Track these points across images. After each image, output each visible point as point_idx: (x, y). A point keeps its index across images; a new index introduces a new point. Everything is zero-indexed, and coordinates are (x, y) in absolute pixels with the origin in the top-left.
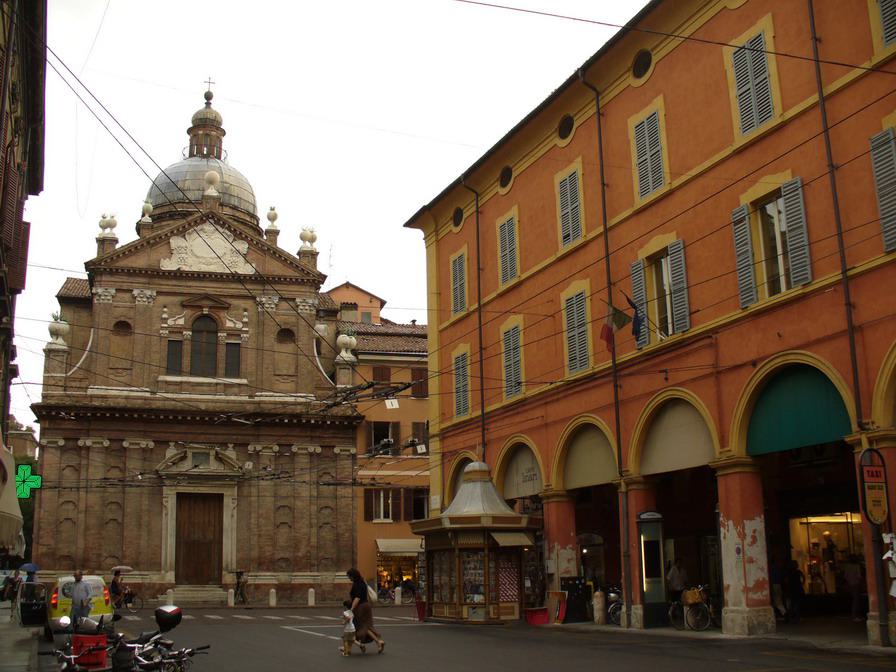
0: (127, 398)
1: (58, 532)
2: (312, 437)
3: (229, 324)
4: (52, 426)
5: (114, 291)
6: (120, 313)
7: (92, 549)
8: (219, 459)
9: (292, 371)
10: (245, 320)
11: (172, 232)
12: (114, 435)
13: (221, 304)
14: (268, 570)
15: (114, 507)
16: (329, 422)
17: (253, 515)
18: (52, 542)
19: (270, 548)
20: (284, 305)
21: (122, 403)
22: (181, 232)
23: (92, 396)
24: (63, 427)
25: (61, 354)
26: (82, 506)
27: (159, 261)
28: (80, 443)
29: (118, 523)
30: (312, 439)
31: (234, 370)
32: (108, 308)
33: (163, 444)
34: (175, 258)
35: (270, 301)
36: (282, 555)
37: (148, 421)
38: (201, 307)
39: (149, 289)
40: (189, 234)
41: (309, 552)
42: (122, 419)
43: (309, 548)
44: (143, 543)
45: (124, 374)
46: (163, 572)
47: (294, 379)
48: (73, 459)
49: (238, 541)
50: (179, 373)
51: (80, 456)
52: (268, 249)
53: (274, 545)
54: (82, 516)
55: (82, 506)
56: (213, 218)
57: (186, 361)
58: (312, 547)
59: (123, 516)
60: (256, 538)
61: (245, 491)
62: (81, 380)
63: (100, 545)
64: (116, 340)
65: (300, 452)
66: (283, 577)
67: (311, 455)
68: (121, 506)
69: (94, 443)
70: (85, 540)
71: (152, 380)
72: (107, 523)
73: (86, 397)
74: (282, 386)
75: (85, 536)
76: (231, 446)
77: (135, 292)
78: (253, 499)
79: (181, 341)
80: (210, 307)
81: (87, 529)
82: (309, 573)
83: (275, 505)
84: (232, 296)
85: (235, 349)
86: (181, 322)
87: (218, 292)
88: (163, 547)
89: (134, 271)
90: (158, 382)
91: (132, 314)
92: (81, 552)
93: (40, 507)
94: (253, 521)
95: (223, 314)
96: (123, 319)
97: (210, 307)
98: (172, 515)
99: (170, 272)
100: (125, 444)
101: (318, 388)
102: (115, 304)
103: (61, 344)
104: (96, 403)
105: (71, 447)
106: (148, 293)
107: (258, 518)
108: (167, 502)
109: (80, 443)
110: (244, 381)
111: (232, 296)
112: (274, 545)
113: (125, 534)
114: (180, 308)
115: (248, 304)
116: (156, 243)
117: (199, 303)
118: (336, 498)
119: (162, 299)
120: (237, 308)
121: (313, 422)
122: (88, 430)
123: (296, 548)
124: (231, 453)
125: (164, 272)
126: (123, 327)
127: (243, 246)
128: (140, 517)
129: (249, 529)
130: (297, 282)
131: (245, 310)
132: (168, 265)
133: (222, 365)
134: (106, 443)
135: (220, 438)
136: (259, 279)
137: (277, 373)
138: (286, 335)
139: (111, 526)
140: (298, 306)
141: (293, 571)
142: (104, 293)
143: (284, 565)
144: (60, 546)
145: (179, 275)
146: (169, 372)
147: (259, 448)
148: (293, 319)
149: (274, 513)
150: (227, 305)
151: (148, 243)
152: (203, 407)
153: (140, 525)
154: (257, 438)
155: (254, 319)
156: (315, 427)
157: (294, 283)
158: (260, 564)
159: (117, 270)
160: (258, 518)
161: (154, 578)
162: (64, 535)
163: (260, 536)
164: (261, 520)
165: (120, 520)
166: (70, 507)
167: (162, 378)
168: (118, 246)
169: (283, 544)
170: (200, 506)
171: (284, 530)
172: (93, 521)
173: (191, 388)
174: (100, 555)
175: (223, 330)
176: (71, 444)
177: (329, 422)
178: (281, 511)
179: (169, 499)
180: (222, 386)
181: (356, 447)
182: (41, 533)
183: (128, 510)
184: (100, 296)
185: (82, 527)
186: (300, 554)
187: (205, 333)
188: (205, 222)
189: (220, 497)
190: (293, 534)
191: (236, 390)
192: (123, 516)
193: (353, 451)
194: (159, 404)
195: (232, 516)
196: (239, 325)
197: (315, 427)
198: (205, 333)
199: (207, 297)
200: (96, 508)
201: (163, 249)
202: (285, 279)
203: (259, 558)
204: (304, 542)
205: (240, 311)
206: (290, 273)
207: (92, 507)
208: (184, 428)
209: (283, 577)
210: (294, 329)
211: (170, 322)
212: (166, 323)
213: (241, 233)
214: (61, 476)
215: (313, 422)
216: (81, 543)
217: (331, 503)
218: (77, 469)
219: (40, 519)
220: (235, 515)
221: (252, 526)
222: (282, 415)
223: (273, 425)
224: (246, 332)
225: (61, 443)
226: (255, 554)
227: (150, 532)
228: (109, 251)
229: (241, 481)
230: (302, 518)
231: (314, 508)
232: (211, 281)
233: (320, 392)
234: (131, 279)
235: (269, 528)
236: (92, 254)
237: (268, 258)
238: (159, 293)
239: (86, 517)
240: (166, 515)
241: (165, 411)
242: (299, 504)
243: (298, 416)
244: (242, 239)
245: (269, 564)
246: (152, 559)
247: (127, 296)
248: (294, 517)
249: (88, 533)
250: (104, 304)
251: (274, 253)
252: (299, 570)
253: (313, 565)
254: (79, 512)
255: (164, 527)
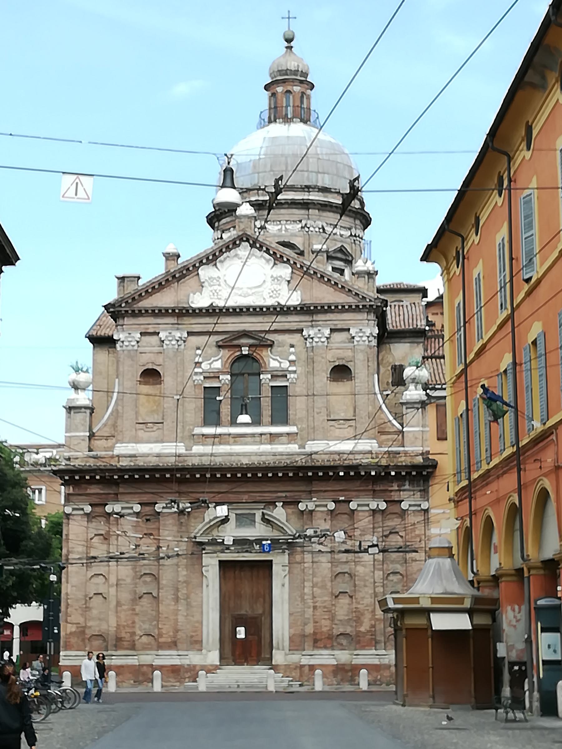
0: (158, 455)
1: (87, 608)
2: (374, 491)
3: (274, 364)
4: (77, 491)
5: (139, 335)
6: (147, 360)
7: (124, 626)
8: (266, 521)
9: (350, 416)
10: (292, 357)
11: (201, 261)
12: (145, 498)
13: (262, 342)
14: (325, 647)
15: (148, 579)
16: (393, 473)
17: (308, 584)
18: (81, 620)
19: (328, 623)
20: (338, 337)
21: (153, 462)
22: (212, 261)
23: (118, 456)
24: (89, 491)
25: (83, 410)
26: (113, 579)
27: (189, 296)
28: (108, 509)
29: (155, 597)
30: (375, 494)
31: (281, 416)
32: (133, 355)
33: (200, 505)
34: (206, 291)
35: (318, 332)
36: (341, 630)
37: (182, 481)
38: (240, 347)
39: (178, 329)
40: (221, 262)
41: (373, 626)
42: (153, 480)
43: (373, 622)
44: (181, 619)
45: (155, 428)
46: (204, 651)
47: (352, 423)
48: (100, 526)
49: (291, 614)
50: (218, 423)
51: (108, 521)
52: (315, 273)
53: (332, 618)
54: (113, 591)
55: (113, 579)
56: (248, 240)
57: (225, 410)
58: (378, 620)
59: (159, 589)
60: (312, 609)
61: (298, 558)
62: (107, 438)
63: (134, 622)
64: (145, 389)
65: (359, 509)
66: (343, 656)
67: (374, 512)
68: (156, 578)
69: (123, 508)
70: (118, 617)
71: (186, 433)
72: (140, 598)
73: (112, 457)
74: (337, 432)
75: (117, 612)
76: (279, 504)
77: (162, 335)
78: (306, 565)
79: (219, 387)
80: (250, 346)
81: (118, 604)
82: (374, 652)
83: (332, 571)
84: (276, 331)
85: (281, 394)
86: (218, 365)
87: (259, 327)
88: (204, 623)
89: (160, 311)
90: (194, 435)
91: (160, 359)
92: (113, 630)
93: (67, 583)
94: (306, 590)
95: (265, 353)
96: (150, 366)
97: (250, 346)
98: (213, 586)
99: (200, 309)
100: (158, 508)
101: (382, 433)
102: (140, 349)
103: (83, 398)
104: (124, 463)
105: (98, 513)
106: (178, 335)
107: (313, 587)
108: (207, 571)
109: (108, 509)
110: (293, 429)
111: (276, 331)
112: (332, 618)
113: (161, 608)
114: (215, 349)
115: (295, 338)
116: (183, 276)
117: (236, 342)
118: (406, 562)
119: (194, 340)
120: (281, 345)
121: (373, 473)
122: (116, 494)
123: (358, 620)
124: (279, 513)
125: (194, 310)
126: (151, 375)
127: (285, 271)
128: (177, 590)
129: (303, 600)
130: (350, 309)
131: (292, 346)
132: (200, 301)
133: (266, 412)
134: (137, 508)
135: (268, 497)
136: (304, 310)
137: (332, 418)
138: (341, 372)
139: (145, 601)
140: (353, 338)
141: (356, 650)
142: (127, 335)
143: (344, 642)
144: (89, 624)
145: (212, 312)
146: (206, 423)
147: (311, 506)
148: (349, 353)
149: (332, 581)
150: (269, 342)
151: (174, 277)
152: (245, 461)
153: (177, 600)
154: (310, 494)
155: (304, 356)
156: (377, 479)
157: (347, 311)
158: (316, 641)
159: (140, 311)
160: (313, 587)
161: (194, 658)
162: (95, 612)
163: (315, 608)
164: (315, 589)
165: (155, 594)
166: (101, 579)
167: (198, 430)
168: (141, 282)
169: (341, 618)
170: (246, 576)
171: (344, 601)
172: (125, 596)
173: (231, 440)
174: (133, 634)
175: (267, 372)
176: (98, 509)
177: (393, 473)
178: (339, 579)
179: (209, 568)
180: (269, 435)
181: (428, 500)
182: (69, 609)
183: (163, 582)
184: (123, 342)
185: (114, 603)
186: (362, 629)
187: (246, 375)
188: (239, 245)
189: (269, 563)
190: (354, 605)
191: (284, 439)
192: (159, 589)
193: (425, 505)
194: (196, 461)
195: (283, 585)
196: (285, 365)
197: (377, 479)
198: (246, 375)
199: (245, 334)
200: (129, 580)
201: (190, 281)
202: (336, 307)
203: (315, 633)
204: (368, 616)
205: (287, 347)
206: (342, 299)
207: (124, 580)
208: (224, 487)
209: (343, 656)
210: (350, 365)
211: (205, 366)
212: (200, 367)
213: (281, 257)
214: (89, 547)
215: (373, 473)
216: (113, 622)
217: (399, 568)
218: (106, 538)
219: (67, 594)
220: (287, 585)
221: (306, 597)
222: (334, 468)
223: (326, 478)
224: (295, 372)
225: (88, 509)
226: (309, 629)
227: (189, 605)
228: (131, 288)
229: (289, 546)
230: (365, 586)
231: (379, 574)
232: (251, 315)
233: (384, 437)
234: (159, 321)
235: (326, 598)
236: (112, 294)
237: (316, 282)
238: (190, 334)
239: (117, 591)
240: (207, 586)
241: (202, 469)
242: (360, 569)
243: (355, 468)
244: (284, 262)
245: (321, 640)
246: (192, 637)
247: (154, 340)
248: (355, 586)
249: (119, 608)
250: (129, 351)
251: (322, 277)
252: (363, 648)
253: (377, 642)
254: (109, 586)
255: (205, 600)
